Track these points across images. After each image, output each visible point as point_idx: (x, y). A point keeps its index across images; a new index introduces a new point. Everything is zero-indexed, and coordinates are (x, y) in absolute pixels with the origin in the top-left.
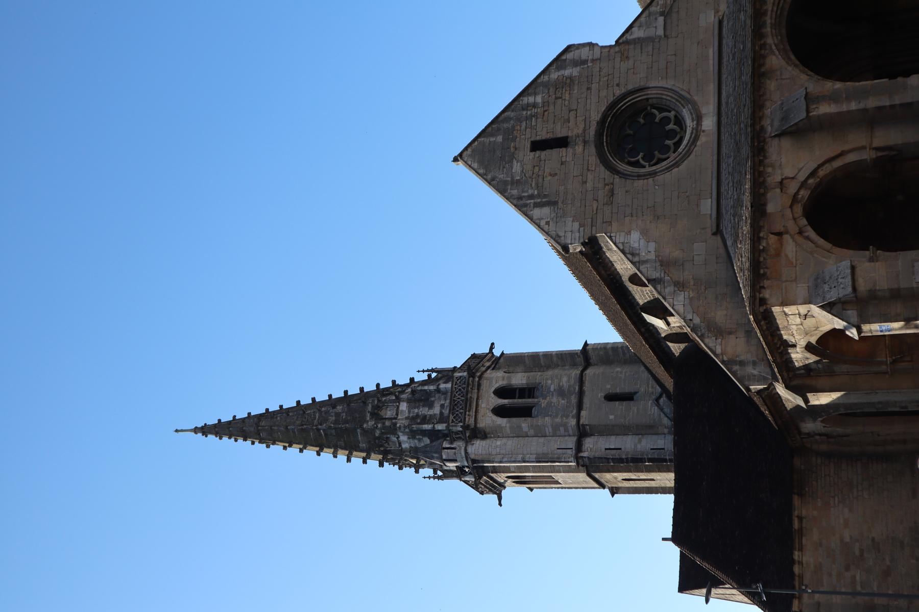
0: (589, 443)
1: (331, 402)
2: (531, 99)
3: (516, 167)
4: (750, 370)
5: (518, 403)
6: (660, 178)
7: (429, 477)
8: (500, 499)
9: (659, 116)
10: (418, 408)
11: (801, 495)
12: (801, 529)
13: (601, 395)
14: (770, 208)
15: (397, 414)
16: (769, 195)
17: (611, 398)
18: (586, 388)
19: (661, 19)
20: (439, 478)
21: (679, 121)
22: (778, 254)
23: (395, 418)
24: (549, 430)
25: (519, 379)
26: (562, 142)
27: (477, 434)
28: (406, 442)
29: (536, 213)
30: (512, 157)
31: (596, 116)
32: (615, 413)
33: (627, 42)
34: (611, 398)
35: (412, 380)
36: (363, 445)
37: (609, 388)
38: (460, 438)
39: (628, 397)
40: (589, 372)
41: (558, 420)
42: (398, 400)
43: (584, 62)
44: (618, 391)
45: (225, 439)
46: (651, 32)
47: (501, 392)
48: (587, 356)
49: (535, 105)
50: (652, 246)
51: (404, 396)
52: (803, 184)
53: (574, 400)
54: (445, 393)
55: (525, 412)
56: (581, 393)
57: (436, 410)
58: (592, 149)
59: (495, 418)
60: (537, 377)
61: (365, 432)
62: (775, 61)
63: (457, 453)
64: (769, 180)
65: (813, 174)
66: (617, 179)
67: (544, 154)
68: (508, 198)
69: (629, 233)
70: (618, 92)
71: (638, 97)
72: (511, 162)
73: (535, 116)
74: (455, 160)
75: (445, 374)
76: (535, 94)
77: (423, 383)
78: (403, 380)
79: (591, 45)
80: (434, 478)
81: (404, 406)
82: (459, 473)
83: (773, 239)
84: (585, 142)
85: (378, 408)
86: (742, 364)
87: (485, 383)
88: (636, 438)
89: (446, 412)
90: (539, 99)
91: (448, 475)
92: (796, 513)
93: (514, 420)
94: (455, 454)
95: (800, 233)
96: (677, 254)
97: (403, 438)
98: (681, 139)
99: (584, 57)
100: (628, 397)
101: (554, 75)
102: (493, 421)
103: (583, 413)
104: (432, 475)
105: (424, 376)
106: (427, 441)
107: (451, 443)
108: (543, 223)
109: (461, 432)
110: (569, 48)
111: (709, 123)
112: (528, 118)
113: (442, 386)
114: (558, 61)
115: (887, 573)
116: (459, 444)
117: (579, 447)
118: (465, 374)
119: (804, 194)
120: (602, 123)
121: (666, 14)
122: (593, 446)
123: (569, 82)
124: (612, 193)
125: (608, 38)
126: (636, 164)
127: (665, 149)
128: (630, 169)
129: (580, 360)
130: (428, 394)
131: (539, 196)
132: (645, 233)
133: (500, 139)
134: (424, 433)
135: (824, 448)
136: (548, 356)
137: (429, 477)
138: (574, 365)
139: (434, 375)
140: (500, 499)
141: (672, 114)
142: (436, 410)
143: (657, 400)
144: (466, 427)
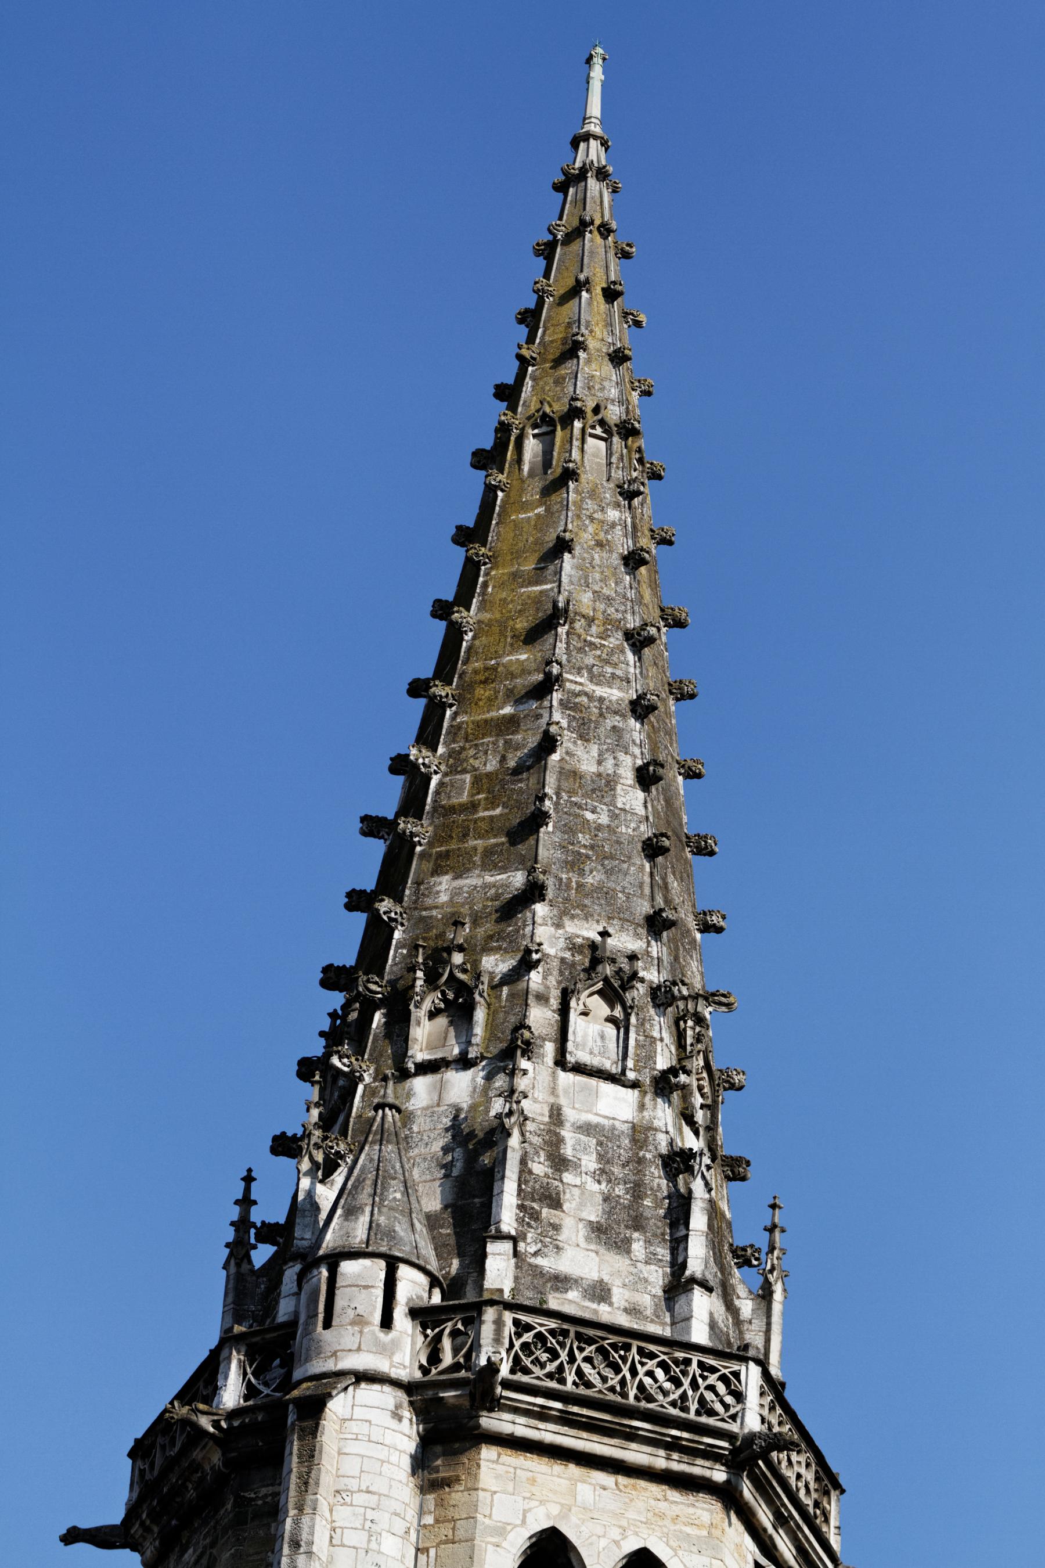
7: (246, 1202)
8: (102, 1538)
10: (602, 1174)
15: (579, 1069)
20: (239, 1250)
23: (561, 1062)
38: (434, 1357)
57: (577, 1257)
80: (242, 1224)
94: (360, 1321)
97: (461, 1086)
102: (501, 1531)
104: (257, 1216)
107: (414, 1313)
109: (468, 1363)
118: (752, 1423)
137: (246, 1202)
140: (102, 1538)
144: (483, 1388)
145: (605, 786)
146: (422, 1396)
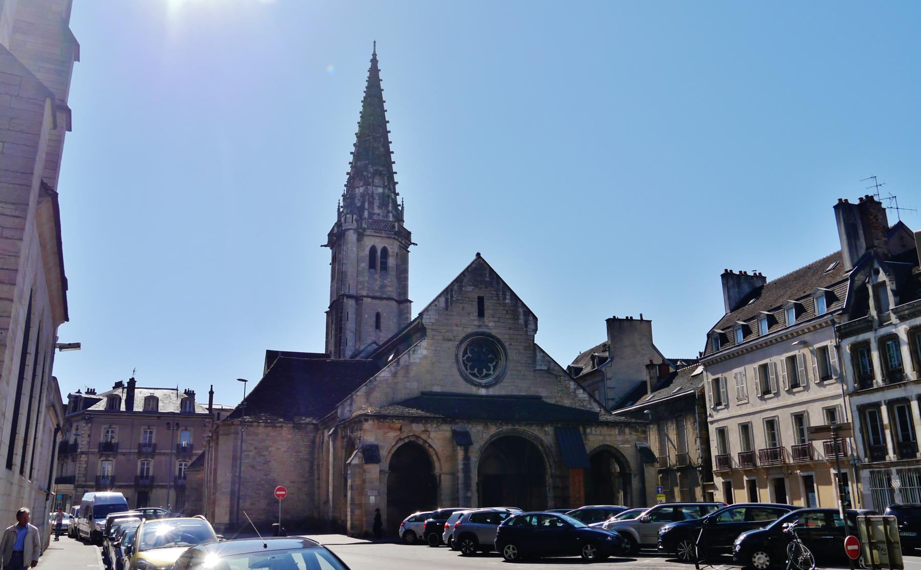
0: (352, 302)
1: (387, 143)
2: (508, 297)
3: (470, 288)
4: (348, 409)
5: (377, 261)
6: (455, 366)
8: (325, 246)
9: (491, 366)
11: (293, 427)
13: (380, 310)
14: (414, 426)
16: (421, 425)
17: (378, 316)
18: (385, 302)
19: (546, 368)
20: (339, 209)
21: (487, 376)
22: (391, 428)
24: (361, 279)
25: (391, 262)
26: (481, 314)
27: (360, 236)
28: (360, 190)
29: (442, 299)
30: (476, 286)
31: (494, 332)
32: (369, 319)
33: (535, 350)
34: (378, 316)
35: (398, 194)
36: (359, 163)
37: (384, 316)
39: (378, 326)
40: (394, 304)
41: (366, 285)
42: (384, 187)
43: (526, 326)
44: (382, 320)
45: (368, 74)
46: (539, 362)
47: (385, 251)
48: (404, 302)
49: (505, 299)
50: (417, 361)
51: (386, 191)
52: (425, 442)
53: (378, 294)
54: (387, 216)
55: (372, 265)
56: (381, 299)
57: (376, 211)
58: (475, 330)
59: (369, 247)
60: (392, 273)
61: (366, 166)
62: (493, 430)
63: (351, 224)
64: (429, 425)
65: (430, 446)
66: (457, 343)
67: (475, 304)
68: (452, 284)
69: (426, 348)
70: (506, 344)
71: (503, 357)
72: (473, 285)
73: (498, 299)
74: (478, 255)
75: (399, 217)
76: (511, 299)
77: (395, 201)
78: (398, 189)
79: (536, 330)
81: (380, 190)
82: (338, 224)
83: (398, 426)
84: (480, 326)
85: (380, 174)
86: (351, 405)
87: (391, 241)
88: (354, 330)
89: (375, 217)
90: (507, 301)
91: (339, 213)
93: (368, 259)
95: (401, 439)
96: (412, 373)
97: (361, 190)
98: (476, 377)
99: (529, 326)
100: (378, 326)
101: (521, 310)
103: (370, 300)
105: (399, 202)
106: (359, 204)
108: (436, 303)
110: (536, 319)
111: (483, 392)
112: (498, 296)
113: (391, 215)
114: (528, 312)
115: (253, 467)
116: (355, 225)
117: (349, 297)
119: (421, 442)
120: (490, 335)
121: (549, 371)
122: (350, 304)
123: (515, 317)
124: (450, 340)
125: (539, 340)
126: (465, 353)
127: (472, 368)
128: (462, 350)
129: (402, 298)
130: (387, 206)
131: (452, 300)
132: (425, 357)
133: (487, 279)
134: (363, 203)
135: (317, 440)
136: (406, 279)
138: (399, 294)
139: (400, 208)
140: (325, 246)
141: (491, 372)
142: (376, 211)
143: (375, 343)
144: (364, 230)
145: (378, 148)
146: (356, 230)
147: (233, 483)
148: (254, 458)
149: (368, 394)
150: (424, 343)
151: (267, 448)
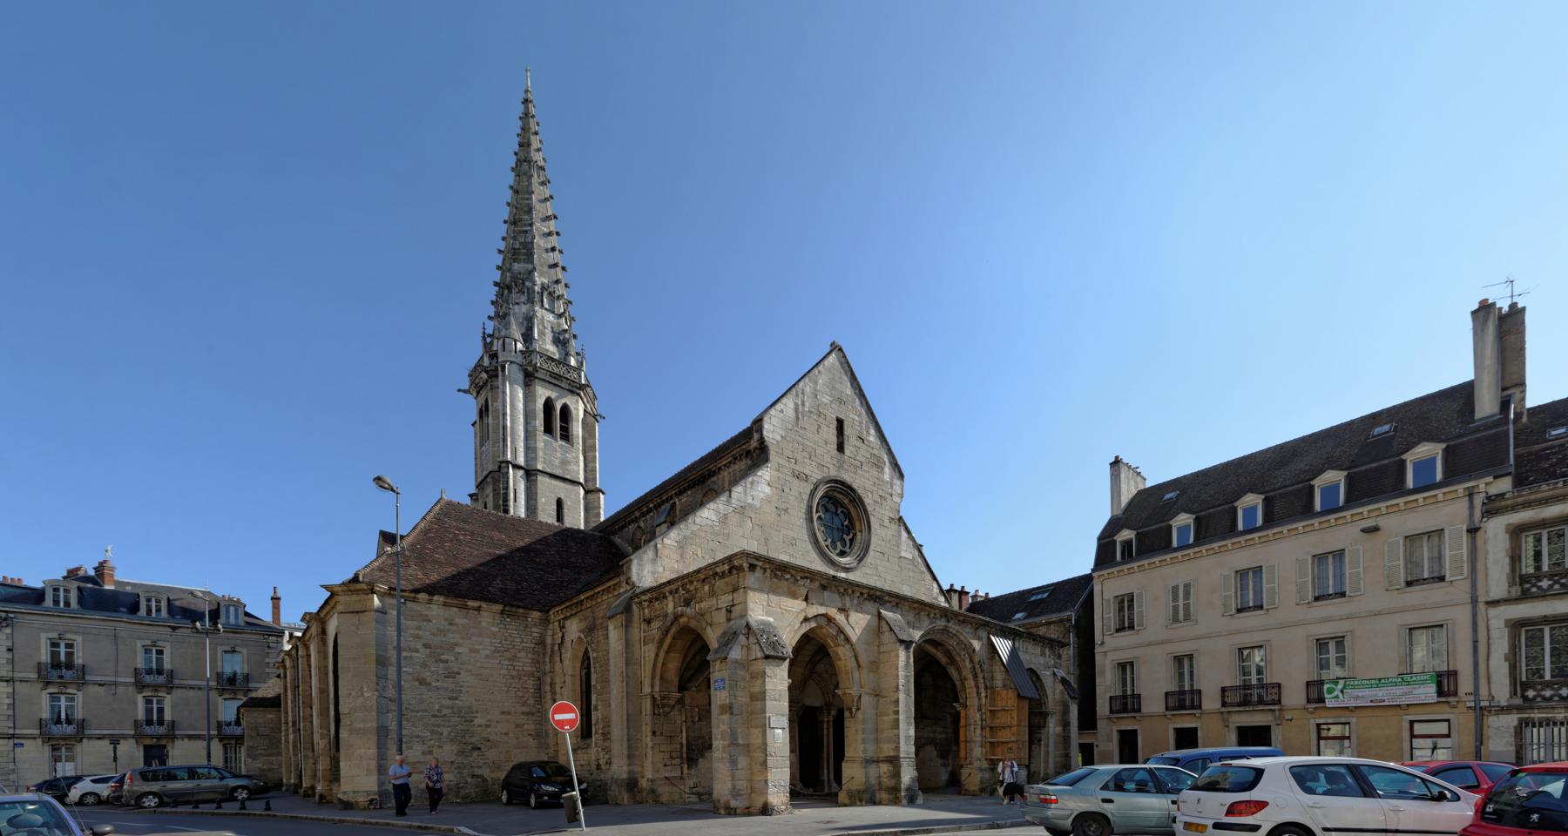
11: (502, 612)
12: (467, 608)
25: (577, 429)
53: (558, 472)
92: (484, 605)
132: (768, 500)
147: (381, 712)
148: (424, 665)
149: (682, 545)
150: (765, 473)
151: (452, 647)
